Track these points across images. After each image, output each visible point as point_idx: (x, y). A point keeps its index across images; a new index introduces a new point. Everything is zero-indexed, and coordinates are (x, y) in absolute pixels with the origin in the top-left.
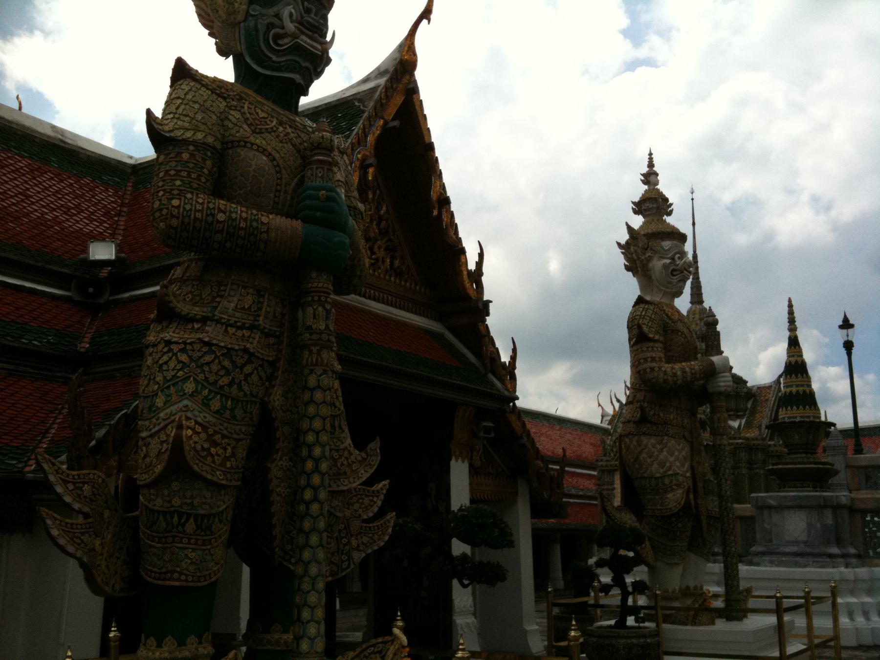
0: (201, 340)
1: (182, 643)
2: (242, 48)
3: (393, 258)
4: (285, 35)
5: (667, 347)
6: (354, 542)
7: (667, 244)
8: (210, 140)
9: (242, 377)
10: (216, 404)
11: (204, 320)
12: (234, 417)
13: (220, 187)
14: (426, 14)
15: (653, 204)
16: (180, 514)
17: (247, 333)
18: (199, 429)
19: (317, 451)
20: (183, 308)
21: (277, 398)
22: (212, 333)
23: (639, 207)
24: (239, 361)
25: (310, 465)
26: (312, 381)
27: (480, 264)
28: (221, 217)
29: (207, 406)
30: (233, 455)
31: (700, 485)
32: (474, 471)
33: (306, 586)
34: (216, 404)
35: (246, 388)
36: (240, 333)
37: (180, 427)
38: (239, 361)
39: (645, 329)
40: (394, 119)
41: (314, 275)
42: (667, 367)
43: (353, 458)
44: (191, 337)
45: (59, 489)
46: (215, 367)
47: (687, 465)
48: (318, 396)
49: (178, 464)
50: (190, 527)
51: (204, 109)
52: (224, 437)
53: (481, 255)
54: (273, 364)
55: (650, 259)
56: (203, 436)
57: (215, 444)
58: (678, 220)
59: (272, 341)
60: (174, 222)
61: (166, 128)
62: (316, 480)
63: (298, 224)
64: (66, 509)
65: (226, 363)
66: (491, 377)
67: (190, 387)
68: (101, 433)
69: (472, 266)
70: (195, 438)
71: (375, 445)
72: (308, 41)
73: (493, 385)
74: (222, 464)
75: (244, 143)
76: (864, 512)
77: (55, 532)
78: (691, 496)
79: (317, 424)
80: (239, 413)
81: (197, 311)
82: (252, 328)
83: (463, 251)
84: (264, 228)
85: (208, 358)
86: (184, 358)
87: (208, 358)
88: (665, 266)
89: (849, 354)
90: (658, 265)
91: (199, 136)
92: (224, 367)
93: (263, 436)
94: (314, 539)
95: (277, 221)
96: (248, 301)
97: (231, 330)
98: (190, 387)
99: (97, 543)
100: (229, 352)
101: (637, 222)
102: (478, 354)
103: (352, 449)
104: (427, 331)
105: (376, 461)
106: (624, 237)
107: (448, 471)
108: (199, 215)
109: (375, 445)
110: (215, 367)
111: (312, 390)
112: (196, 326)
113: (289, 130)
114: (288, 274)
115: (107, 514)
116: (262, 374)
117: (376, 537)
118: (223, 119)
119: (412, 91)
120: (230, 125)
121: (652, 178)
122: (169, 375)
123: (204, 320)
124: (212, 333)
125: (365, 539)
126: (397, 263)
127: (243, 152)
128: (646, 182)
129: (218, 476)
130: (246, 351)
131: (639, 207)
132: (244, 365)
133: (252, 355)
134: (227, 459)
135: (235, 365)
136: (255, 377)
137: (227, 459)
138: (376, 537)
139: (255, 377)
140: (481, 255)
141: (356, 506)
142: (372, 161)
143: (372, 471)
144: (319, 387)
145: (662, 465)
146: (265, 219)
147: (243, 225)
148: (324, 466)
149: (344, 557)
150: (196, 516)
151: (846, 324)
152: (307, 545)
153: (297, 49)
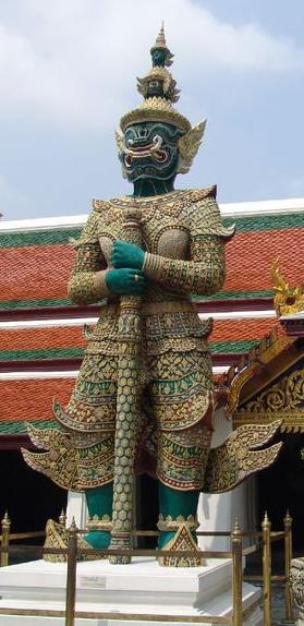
38: (98, 360)
43: (193, 408)
52: (85, 405)
115: (63, 450)
125: (250, 462)
129: (82, 428)
130: (100, 354)
133: (104, 355)
139: (108, 368)
153: (136, 160)
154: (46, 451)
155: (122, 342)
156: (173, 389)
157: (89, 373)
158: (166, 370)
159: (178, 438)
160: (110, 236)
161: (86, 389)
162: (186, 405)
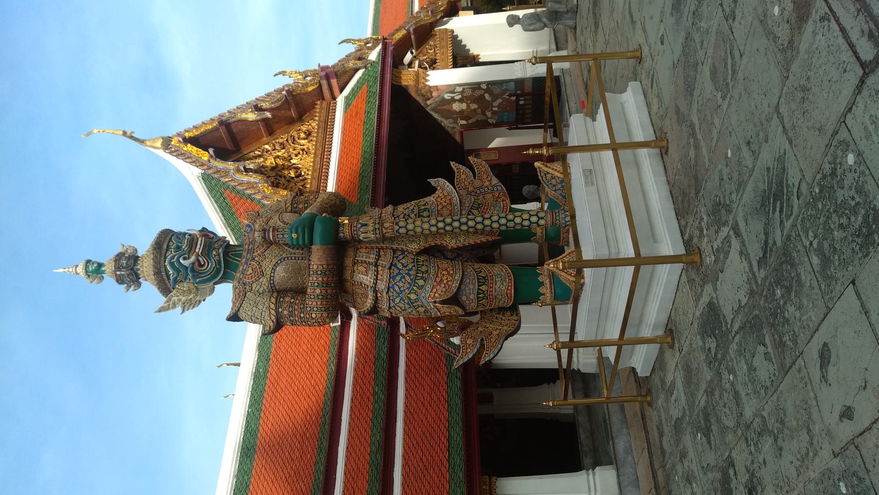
0: (387, 292)
1: (542, 284)
2: (211, 284)
4: (198, 260)
6: (487, 183)
8: (273, 300)
9: (405, 269)
11: (375, 291)
12: (427, 271)
16: (478, 293)
17: (380, 268)
18: (435, 290)
20: (369, 303)
21: (414, 247)
22: (382, 286)
24: (396, 271)
25: (448, 228)
28: (318, 291)
29: (422, 287)
30: (446, 270)
33: (511, 224)
34: (421, 282)
35: (410, 266)
36: (381, 272)
37: (435, 302)
38: (396, 271)
41: (342, 235)
45: (471, 356)
46: (401, 284)
50: (484, 288)
52: (437, 276)
54: (394, 251)
56: (438, 287)
57: (442, 280)
59: (382, 253)
60: (325, 315)
61: (272, 324)
64: (479, 353)
65: (398, 278)
70: (440, 292)
71: (433, 181)
72: (198, 246)
74: (451, 275)
75: (271, 281)
77: (492, 356)
79: (426, 226)
80: (424, 269)
82: (376, 265)
84: (320, 267)
85: (397, 288)
86: (397, 300)
87: (397, 288)
91: (273, 306)
92: (400, 280)
93: (433, 252)
96: (362, 269)
97: (379, 277)
99: (495, 333)
103: (436, 195)
105: (442, 181)
107: (436, 88)
108: (319, 303)
109: (433, 181)
110: (401, 284)
111: (408, 231)
112: (379, 295)
113: (256, 254)
116: (401, 257)
117: (483, 169)
120: (262, 289)
122: (407, 306)
123: (375, 291)
124: (382, 286)
127: (277, 279)
129: (458, 277)
130: (390, 268)
132: (398, 268)
133: (391, 264)
134: (448, 273)
135: (399, 274)
136: (404, 261)
137: (448, 273)
138: (483, 169)
141: (467, 183)
143: (448, 183)
144: (405, 227)
146: (315, 267)
147: (320, 279)
149: (495, 189)
150: (479, 286)
152: (491, 226)
154: (482, 340)
155: (382, 226)
156: (425, 210)
157: (407, 278)
158: (409, 215)
159: (467, 205)
160: (277, 264)
161: (422, 278)
162: (439, 200)
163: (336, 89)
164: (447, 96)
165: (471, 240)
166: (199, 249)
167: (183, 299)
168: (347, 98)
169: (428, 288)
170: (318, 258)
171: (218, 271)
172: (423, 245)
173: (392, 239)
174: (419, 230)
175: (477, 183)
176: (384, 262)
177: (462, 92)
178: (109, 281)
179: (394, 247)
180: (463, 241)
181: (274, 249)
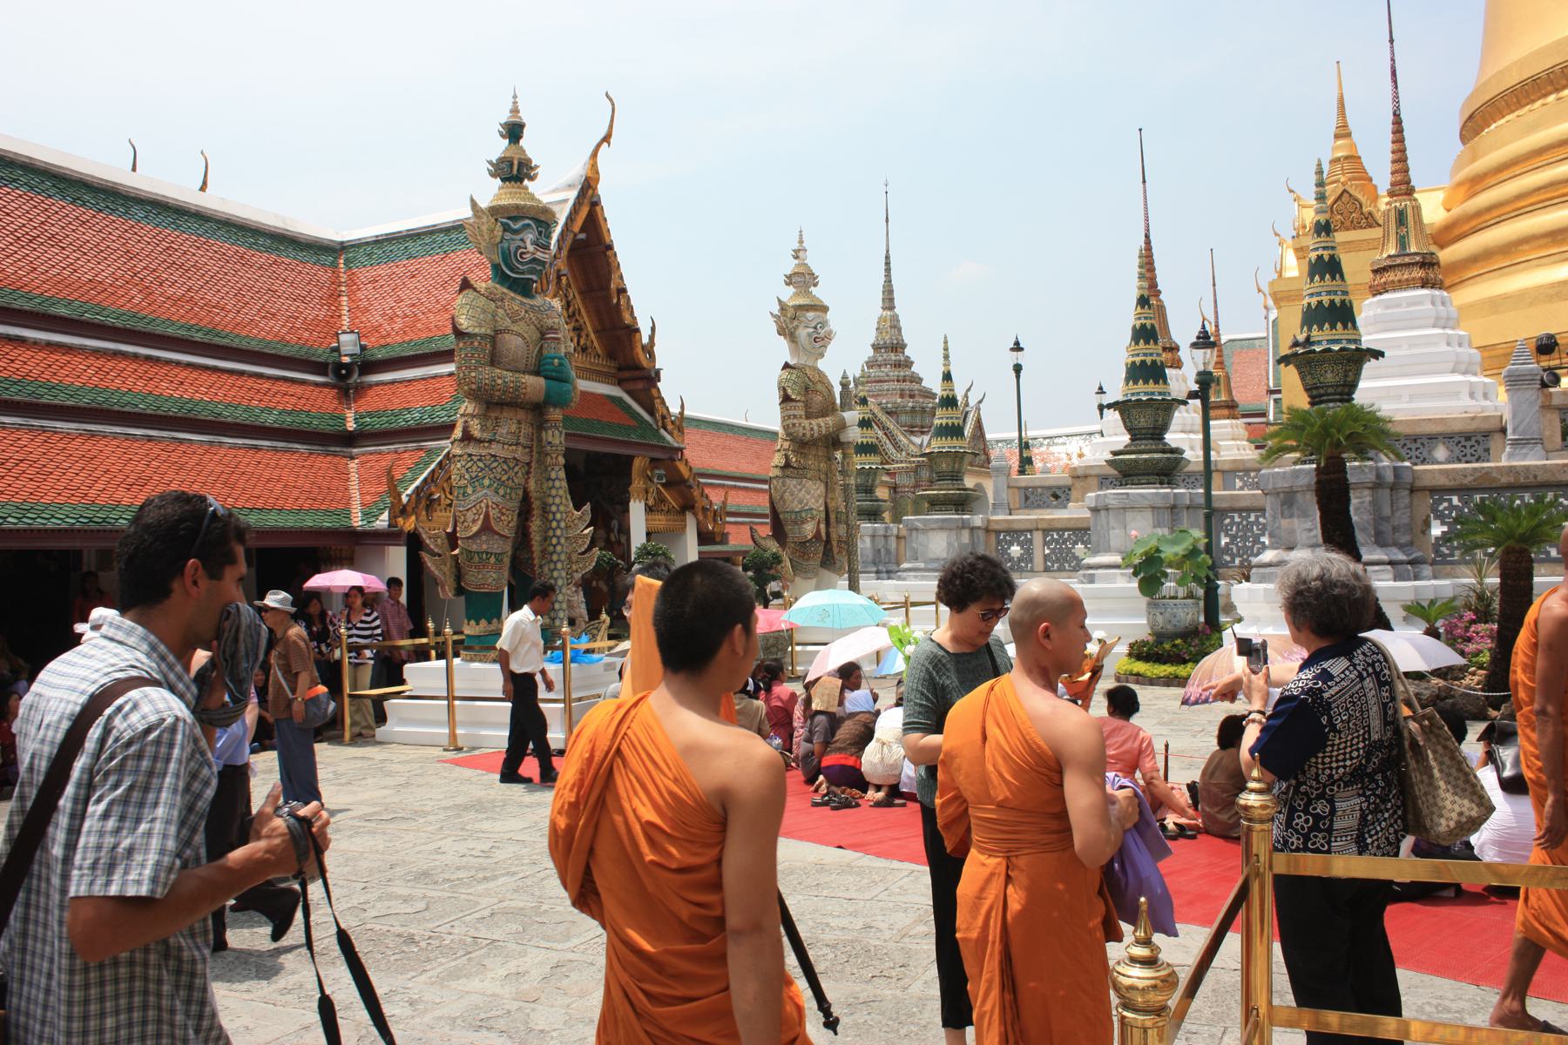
3: (579, 336)
5: (807, 405)
7: (810, 315)
10: (502, 492)
11: (490, 441)
13: (494, 360)
14: (607, 139)
15: (802, 278)
19: (558, 516)
20: (477, 434)
21: (532, 485)
22: (495, 449)
23: (790, 280)
26: (553, 475)
27: (652, 338)
31: (833, 516)
32: (649, 510)
34: (502, 492)
39: (789, 391)
40: (582, 231)
42: (806, 423)
44: (484, 452)
47: (821, 501)
48: (557, 484)
49: (486, 528)
50: (492, 560)
51: (484, 311)
53: (653, 329)
55: (796, 328)
58: (820, 293)
62: (558, 532)
63: (541, 380)
66: (662, 431)
67: (486, 482)
68: (405, 499)
69: (645, 340)
71: (587, 507)
73: (664, 439)
76: (998, 532)
78: (822, 526)
79: (557, 500)
81: (486, 436)
83: (638, 330)
88: (809, 335)
89: (1018, 377)
90: (803, 333)
91: (483, 330)
94: (559, 565)
95: (530, 380)
96: (514, 428)
98: (486, 482)
100: (506, 460)
101: (787, 294)
102: (651, 411)
104: (609, 397)
105: (588, 518)
106: (776, 310)
107: (628, 511)
109: (587, 507)
114: (537, 410)
118: (494, 315)
119: (595, 204)
121: (801, 254)
123: (490, 441)
124: (495, 449)
126: (582, 342)
128: (796, 257)
129: (506, 532)
131: (790, 280)
140: (653, 329)
142: (564, 270)
145: (800, 502)
148: (563, 525)
151: (1017, 347)
153: (535, 260)
163: (631, 386)
164: (615, 523)
165: (536, 548)
166: (539, 255)
167: (484, 228)
168: (620, 400)
169: (497, 499)
170: (534, 384)
171: (512, 270)
172: (534, 495)
173: (540, 462)
174: (554, 492)
175: (574, 557)
176: (520, 453)
177: (619, 543)
178: (500, 147)
179: (533, 464)
180: (536, 538)
181: (536, 335)
